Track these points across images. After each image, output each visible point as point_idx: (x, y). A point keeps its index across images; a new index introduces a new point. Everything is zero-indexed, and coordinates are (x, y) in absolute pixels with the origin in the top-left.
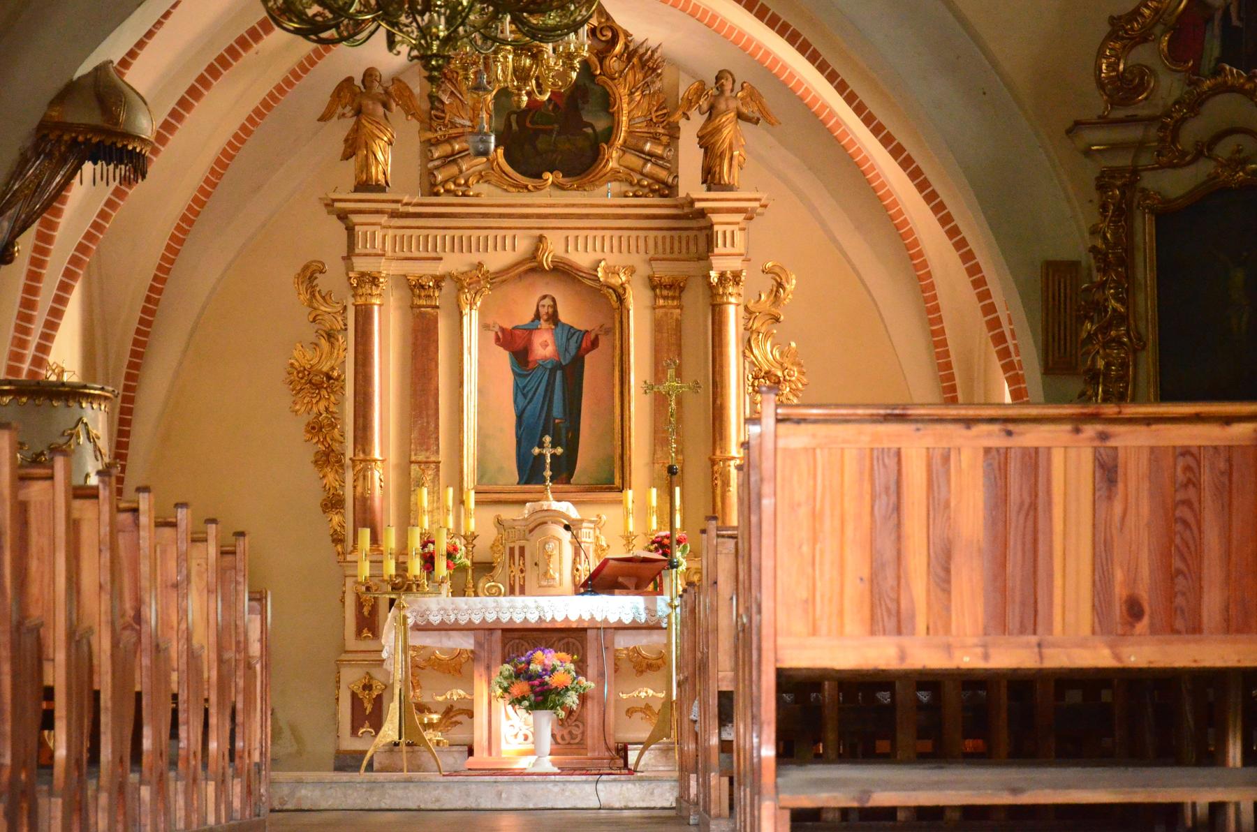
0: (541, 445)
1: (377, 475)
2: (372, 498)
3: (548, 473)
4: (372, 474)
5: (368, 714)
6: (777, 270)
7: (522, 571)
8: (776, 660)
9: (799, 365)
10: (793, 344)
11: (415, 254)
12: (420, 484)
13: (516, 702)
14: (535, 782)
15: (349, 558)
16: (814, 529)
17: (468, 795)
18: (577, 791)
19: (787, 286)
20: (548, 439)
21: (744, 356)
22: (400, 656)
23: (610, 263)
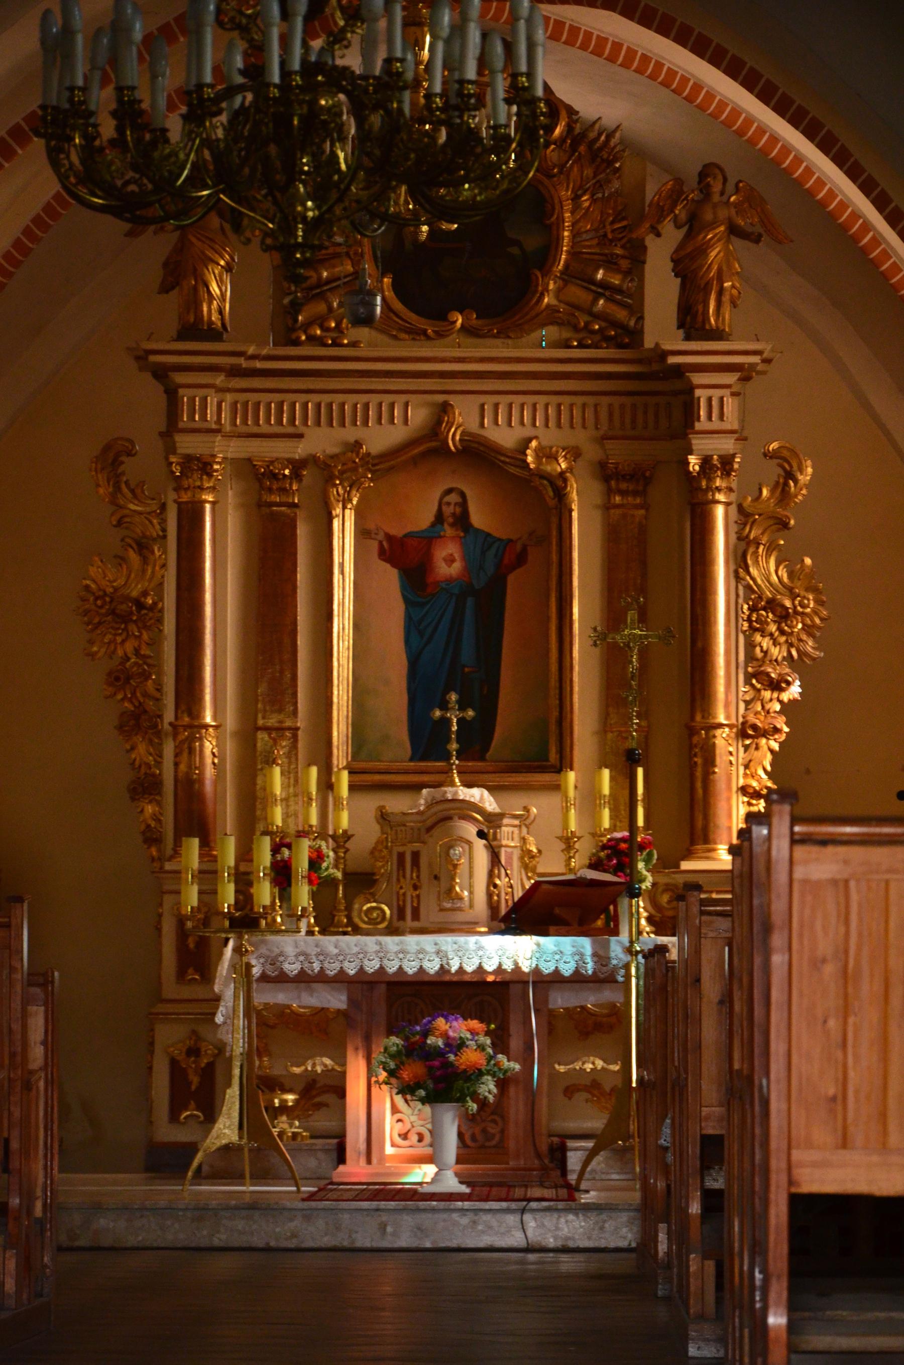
0: (444, 706)
1: (208, 747)
2: (201, 780)
3: (454, 746)
4: (202, 746)
5: (198, 1093)
6: (786, 453)
7: (415, 887)
8: (791, 1182)
9: (815, 590)
10: (808, 561)
11: (265, 429)
12: (271, 761)
13: (407, 1090)
14: (434, 1210)
15: (168, 866)
16: (846, 995)
17: (338, 1229)
18: (494, 1223)
19: (800, 477)
20: (454, 697)
21: (738, 578)
22: (241, 1022)
23: (545, 443)
